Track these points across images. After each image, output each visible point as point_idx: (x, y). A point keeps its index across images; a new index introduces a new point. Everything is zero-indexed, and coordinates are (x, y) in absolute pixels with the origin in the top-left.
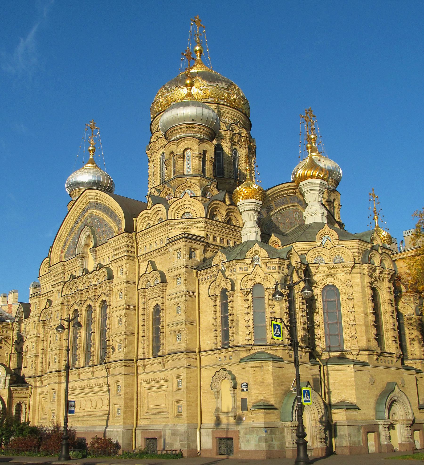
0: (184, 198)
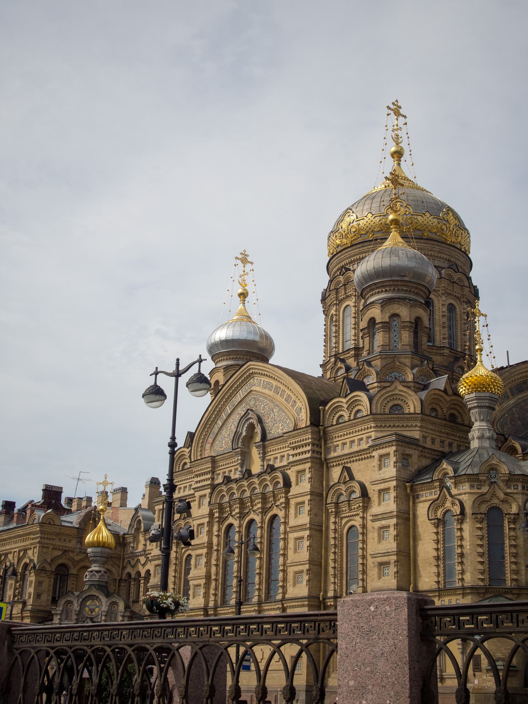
0: (393, 387)
